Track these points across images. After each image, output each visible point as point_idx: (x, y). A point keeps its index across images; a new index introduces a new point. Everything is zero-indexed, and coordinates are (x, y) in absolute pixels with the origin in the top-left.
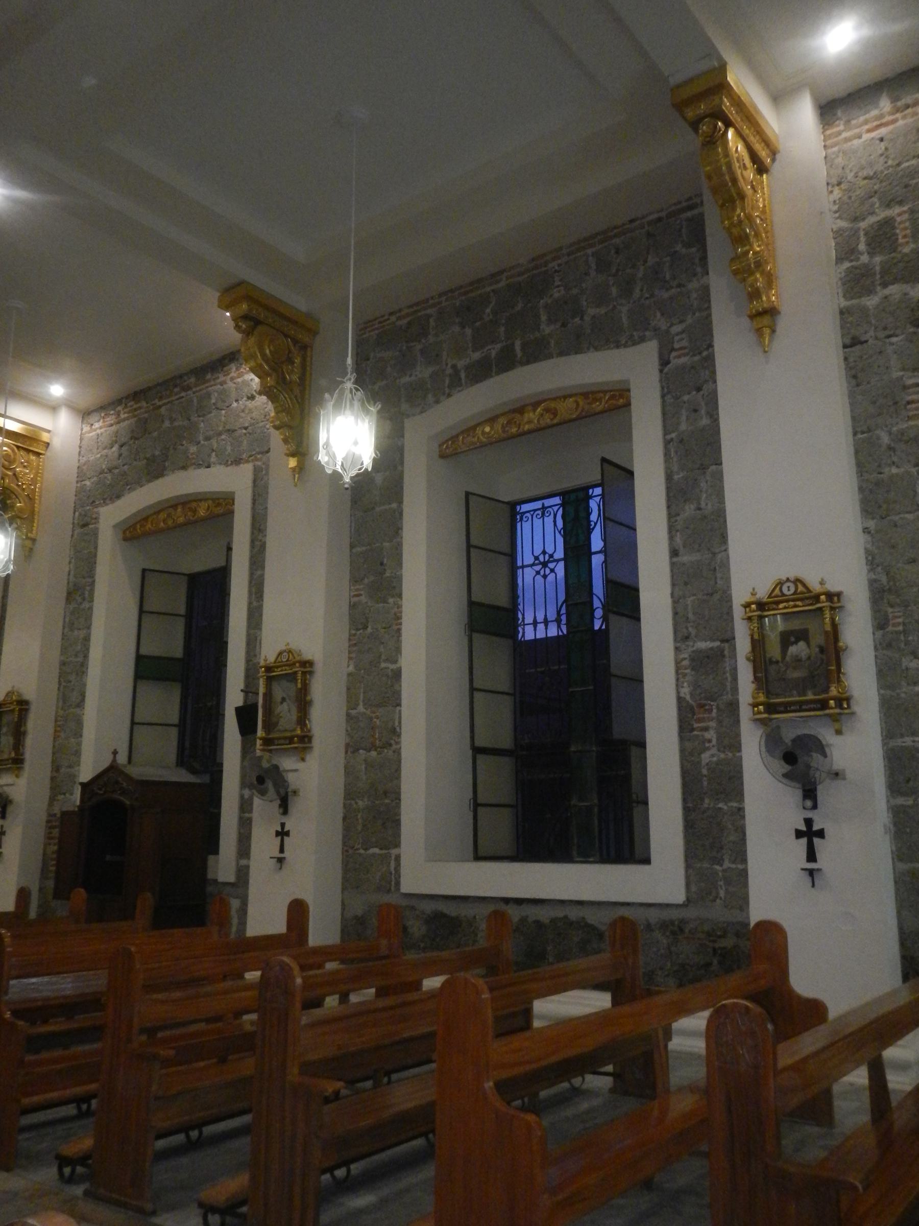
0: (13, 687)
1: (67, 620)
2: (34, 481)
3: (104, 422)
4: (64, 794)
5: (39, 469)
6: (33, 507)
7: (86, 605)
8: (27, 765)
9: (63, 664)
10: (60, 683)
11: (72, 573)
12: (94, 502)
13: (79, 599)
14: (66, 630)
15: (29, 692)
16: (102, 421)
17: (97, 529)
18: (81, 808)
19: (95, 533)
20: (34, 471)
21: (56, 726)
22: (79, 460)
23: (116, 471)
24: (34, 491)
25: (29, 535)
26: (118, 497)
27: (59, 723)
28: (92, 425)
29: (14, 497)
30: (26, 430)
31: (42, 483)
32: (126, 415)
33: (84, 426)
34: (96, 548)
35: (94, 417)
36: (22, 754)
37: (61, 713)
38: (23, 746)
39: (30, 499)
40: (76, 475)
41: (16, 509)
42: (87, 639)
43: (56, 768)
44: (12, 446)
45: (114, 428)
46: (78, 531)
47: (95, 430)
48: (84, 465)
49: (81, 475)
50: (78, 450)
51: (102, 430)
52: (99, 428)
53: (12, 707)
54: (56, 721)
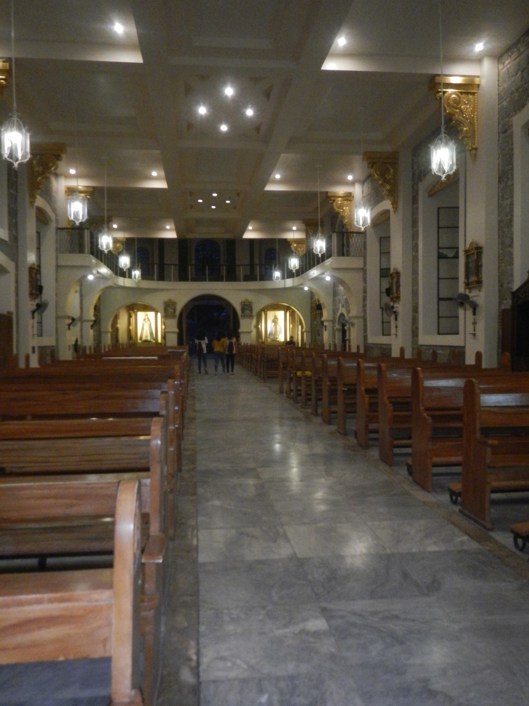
0: (473, 240)
1: (500, 194)
2: (473, 112)
3: (511, 58)
4: (506, 300)
5: (475, 103)
6: (474, 128)
7: (510, 183)
8: (484, 284)
9: (500, 222)
10: (499, 235)
11: (500, 165)
12: (509, 114)
13: (505, 180)
14: (500, 201)
15: (482, 241)
16: (509, 58)
17: (512, 132)
18: (513, 307)
19: (511, 136)
20: (472, 105)
21: (499, 260)
22: (498, 90)
23: (521, 89)
24: (473, 118)
25: (473, 146)
26: (523, 106)
27: (501, 258)
28: (504, 63)
29: (462, 125)
30: (464, 80)
31: (478, 112)
32: (524, 48)
33: (499, 66)
34: (512, 144)
35: (505, 56)
36: (481, 278)
37: (501, 252)
38: (481, 274)
39: (472, 123)
40: (498, 100)
41: (463, 132)
42: (512, 204)
43: (501, 285)
44: (457, 93)
45: (517, 60)
46: (502, 136)
47: (506, 66)
48: (502, 91)
49: (501, 98)
50: (497, 83)
51: (511, 64)
52: (508, 63)
53: (473, 251)
54: (499, 257)
